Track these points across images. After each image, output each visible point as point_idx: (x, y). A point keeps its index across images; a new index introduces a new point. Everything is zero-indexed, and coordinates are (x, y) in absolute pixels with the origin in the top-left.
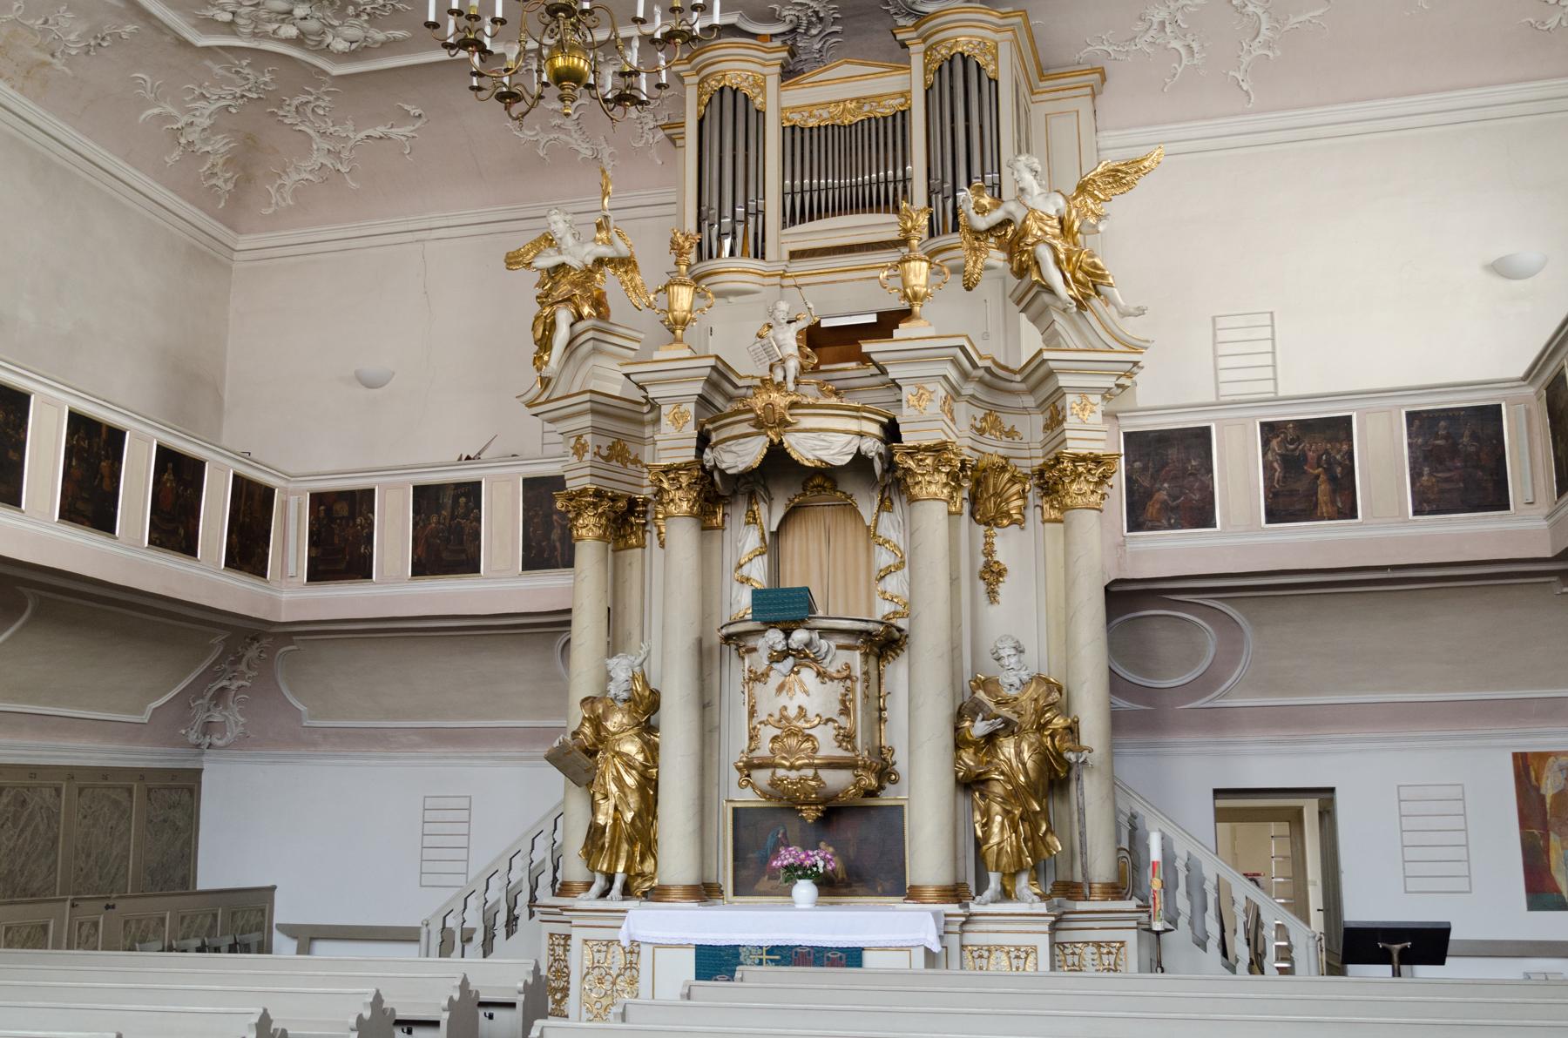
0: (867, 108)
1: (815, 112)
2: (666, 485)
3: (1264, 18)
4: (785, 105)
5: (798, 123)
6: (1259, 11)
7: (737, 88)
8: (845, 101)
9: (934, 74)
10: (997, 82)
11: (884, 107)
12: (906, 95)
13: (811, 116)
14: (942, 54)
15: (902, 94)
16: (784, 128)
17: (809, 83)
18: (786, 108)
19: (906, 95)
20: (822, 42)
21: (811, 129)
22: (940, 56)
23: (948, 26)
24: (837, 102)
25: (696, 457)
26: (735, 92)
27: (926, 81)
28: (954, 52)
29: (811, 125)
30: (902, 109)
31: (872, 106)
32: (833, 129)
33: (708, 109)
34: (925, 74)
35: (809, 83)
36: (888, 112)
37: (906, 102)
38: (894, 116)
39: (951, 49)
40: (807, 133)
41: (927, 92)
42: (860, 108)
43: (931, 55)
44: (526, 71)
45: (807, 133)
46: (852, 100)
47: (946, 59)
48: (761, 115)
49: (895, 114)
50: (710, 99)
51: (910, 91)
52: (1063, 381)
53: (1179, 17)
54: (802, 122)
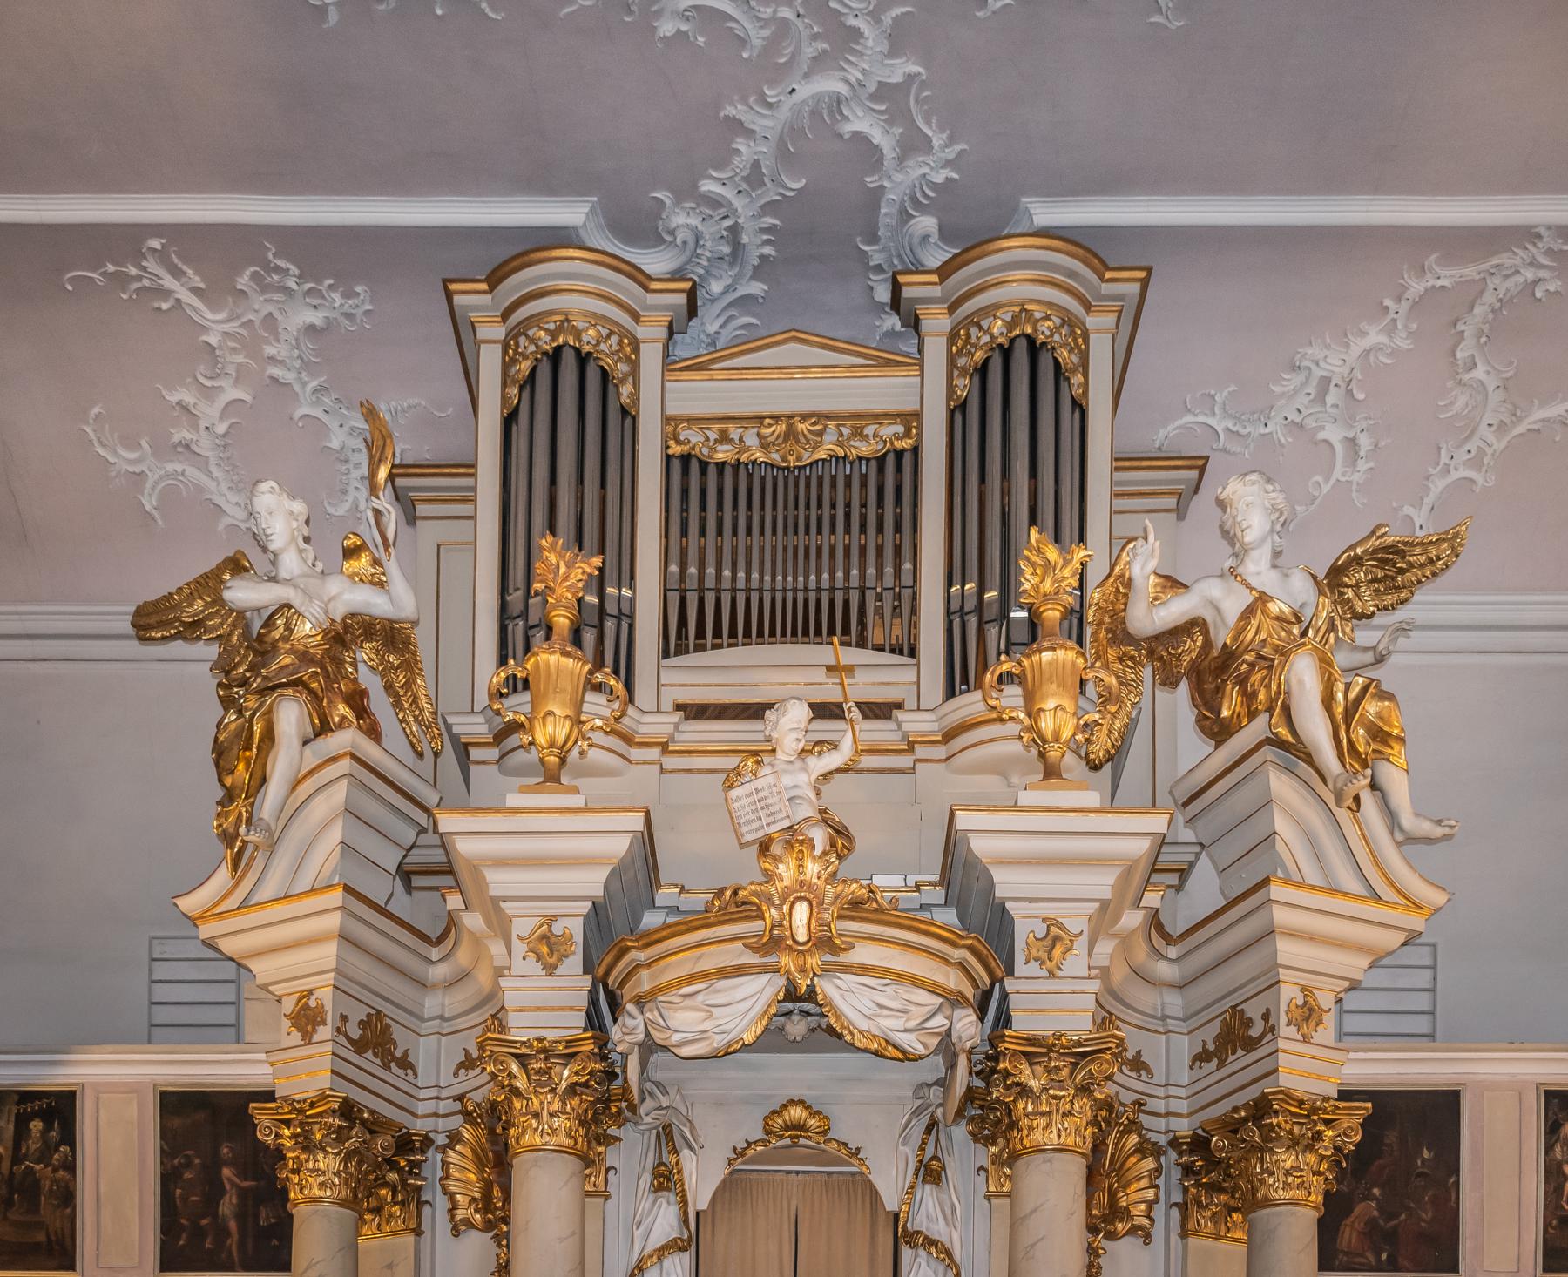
0: (830, 437)
1: (734, 434)
2: (521, 1083)
3: (1495, 397)
4: (670, 412)
6: (1491, 383)
8: (792, 417)
12: (910, 420)
13: (724, 438)
16: (669, 458)
18: (674, 419)
19: (910, 420)
20: (721, 320)
24: (777, 418)
25: (585, 1030)
30: (899, 445)
31: (841, 434)
36: (865, 449)
37: (907, 434)
38: (881, 460)
40: (712, 471)
42: (820, 434)
44: (138, 290)
45: (712, 471)
46: (804, 417)
48: (628, 421)
49: (885, 455)
52: (1287, 950)
53: (1358, 374)
54: (705, 451)
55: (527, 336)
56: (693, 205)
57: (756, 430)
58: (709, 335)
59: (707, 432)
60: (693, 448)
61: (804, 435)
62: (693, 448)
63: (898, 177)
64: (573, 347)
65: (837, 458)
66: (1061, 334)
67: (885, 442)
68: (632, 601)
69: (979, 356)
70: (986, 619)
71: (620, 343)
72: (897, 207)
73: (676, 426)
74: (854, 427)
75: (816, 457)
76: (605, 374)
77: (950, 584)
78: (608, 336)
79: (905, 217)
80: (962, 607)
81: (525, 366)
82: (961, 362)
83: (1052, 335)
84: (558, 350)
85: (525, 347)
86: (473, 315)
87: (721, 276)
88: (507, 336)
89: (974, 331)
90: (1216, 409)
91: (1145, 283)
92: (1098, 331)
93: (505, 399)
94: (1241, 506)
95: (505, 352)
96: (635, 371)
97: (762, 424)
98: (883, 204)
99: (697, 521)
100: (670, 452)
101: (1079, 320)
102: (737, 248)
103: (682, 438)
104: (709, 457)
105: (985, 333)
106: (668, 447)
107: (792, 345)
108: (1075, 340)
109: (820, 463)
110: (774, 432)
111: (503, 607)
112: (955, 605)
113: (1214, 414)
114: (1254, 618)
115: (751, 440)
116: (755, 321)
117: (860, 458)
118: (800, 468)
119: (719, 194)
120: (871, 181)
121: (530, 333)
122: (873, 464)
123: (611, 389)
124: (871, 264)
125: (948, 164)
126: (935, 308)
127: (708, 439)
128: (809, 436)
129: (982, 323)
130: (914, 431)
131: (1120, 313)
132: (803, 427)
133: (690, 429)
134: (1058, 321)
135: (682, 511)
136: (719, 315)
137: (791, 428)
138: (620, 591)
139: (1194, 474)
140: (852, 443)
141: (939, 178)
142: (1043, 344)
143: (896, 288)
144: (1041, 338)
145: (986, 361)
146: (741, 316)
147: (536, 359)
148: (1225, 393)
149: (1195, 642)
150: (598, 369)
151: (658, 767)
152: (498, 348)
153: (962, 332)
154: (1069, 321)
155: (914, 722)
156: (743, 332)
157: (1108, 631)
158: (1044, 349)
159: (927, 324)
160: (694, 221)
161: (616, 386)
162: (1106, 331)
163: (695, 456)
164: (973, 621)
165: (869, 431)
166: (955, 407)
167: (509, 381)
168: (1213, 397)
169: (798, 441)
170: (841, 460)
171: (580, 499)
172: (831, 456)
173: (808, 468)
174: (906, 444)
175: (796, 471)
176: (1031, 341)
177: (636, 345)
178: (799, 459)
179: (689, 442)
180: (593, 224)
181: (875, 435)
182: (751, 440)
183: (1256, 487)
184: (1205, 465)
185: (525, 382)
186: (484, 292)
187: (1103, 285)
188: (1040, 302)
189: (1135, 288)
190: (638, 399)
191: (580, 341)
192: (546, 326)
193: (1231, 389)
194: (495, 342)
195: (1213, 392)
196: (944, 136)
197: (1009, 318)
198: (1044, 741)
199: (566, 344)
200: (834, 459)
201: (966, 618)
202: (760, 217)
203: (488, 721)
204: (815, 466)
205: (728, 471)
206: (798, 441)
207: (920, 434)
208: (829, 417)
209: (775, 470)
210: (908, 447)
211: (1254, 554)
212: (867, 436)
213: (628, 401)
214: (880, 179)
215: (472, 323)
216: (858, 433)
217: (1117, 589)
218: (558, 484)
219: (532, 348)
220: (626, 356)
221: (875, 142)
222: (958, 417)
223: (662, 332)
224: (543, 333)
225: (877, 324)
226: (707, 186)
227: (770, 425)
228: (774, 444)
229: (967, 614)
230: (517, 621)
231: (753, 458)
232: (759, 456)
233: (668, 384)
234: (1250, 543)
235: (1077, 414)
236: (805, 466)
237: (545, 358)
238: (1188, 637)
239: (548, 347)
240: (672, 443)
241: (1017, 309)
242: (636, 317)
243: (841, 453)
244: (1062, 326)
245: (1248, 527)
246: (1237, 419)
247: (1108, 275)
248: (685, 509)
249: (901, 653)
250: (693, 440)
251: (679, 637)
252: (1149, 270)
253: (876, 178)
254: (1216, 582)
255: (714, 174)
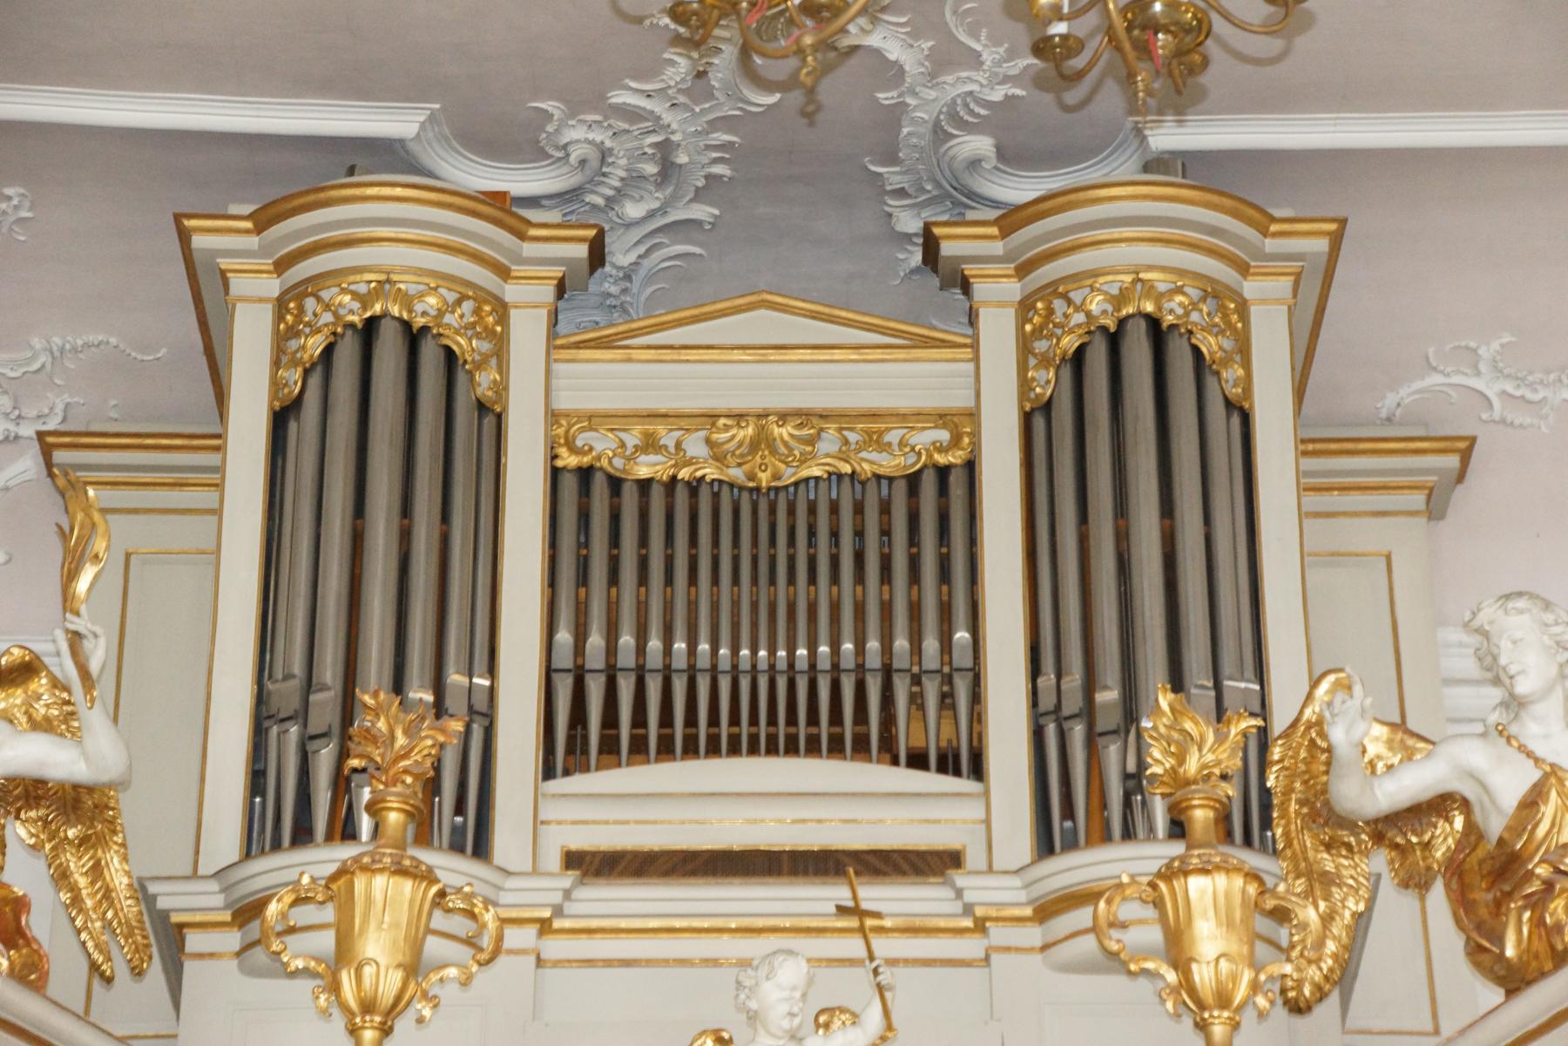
0: (829, 443)
1: (669, 440)
4: (563, 402)
5: (604, 463)
7: (425, 329)
9: (1058, 368)
10: (1246, 419)
11: (885, 447)
13: (650, 444)
14: (1088, 314)
15: (942, 418)
16: (555, 474)
17: (649, 347)
21: (645, 485)
22: (1079, 318)
23: (1116, 232)
24: (739, 417)
26: (413, 337)
27: (1025, 385)
28: (1129, 310)
29: (643, 472)
30: (941, 459)
31: (846, 442)
32: (716, 496)
33: (315, 380)
34: (1023, 367)
35: (649, 347)
36: (889, 463)
37: (956, 441)
38: (913, 481)
39: (1119, 300)
41: (1027, 419)
42: (811, 441)
43: (1050, 312)
46: (783, 417)
47: (1104, 329)
49: (920, 471)
50: (329, 351)
51: (973, 415)
54: (618, 462)
55: (319, 299)
56: (598, 118)
57: (702, 434)
58: (619, 268)
59: (622, 435)
60: (599, 458)
61: (785, 444)
62: (599, 458)
63: (933, 94)
64: (400, 320)
65: (840, 476)
66: (1201, 311)
67: (919, 454)
68: (492, 691)
69: (1070, 343)
70: (1100, 728)
71: (477, 311)
72: (930, 126)
73: (570, 426)
74: (869, 433)
75: (805, 473)
76: (450, 355)
77: (1035, 670)
78: (459, 302)
79: (940, 135)
80: (1058, 706)
81: (314, 345)
82: (1041, 346)
83: (1187, 314)
84: (371, 325)
85: (315, 315)
86: (224, 263)
87: (642, 197)
88: (283, 294)
89: (1058, 304)
90: (1483, 367)
91: (1336, 240)
92: (1263, 301)
93: (276, 384)
94: (1505, 644)
95: (279, 317)
96: (501, 348)
97: (713, 424)
98: (904, 123)
99: (605, 561)
100: (559, 463)
101: (1228, 287)
102: (668, 170)
103: (579, 443)
104: (624, 471)
105: (1078, 309)
106: (555, 457)
107: (762, 312)
108: (1225, 317)
109: (812, 483)
110: (733, 437)
111: (261, 698)
112: (1047, 702)
113: (1478, 374)
114: (1546, 802)
115: (695, 446)
116: (697, 250)
117: (878, 477)
118: (777, 489)
119: (639, 107)
120: (886, 97)
121: (325, 295)
122: (900, 489)
123: (461, 378)
124: (889, 188)
125: (1006, 79)
126: (992, 269)
127: (623, 445)
128: (792, 443)
129: (1072, 295)
130: (966, 440)
131: (1298, 277)
132: (783, 432)
133: (591, 429)
134: (1194, 293)
135: (579, 546)
136: (636, 244)
137: (761, 430)
138: (471, 677)
139: (1453, 461)
140: (864, 454)
141: (997, 95)
142: (1172, 327)
143: (930, 245)
144: (1169, 319)
145: (1080, 352)
146: (674, 243)
147: (334, 334)
148: (1495, 346)
149: (1451, 823)
150: (442, 354)
151: (532, 959)
152: (267, 313)
153: (1039, 305)
154: (1214, 292)
155: (979, 889)
156: (679, 263)
157: (1301, 803)
158: (1176, 333)
159: (980, 289)
160: (597, 136)
161: (470, 373)
162: (1278, 301)
163: (601, 469)
164: (1078, 731)
165: (893, 437)
166: (1033, 410)
167: (284, 359)
168: (1475, 351)
169: (774, 452)
170: (847, 481)
171: (405, 537)
172: (830, 474)
173: (792, 489)
174: (955, 458)
175: (772, 495)
176: (1153, 323)
177: (502, 309)
178: (776, 476)
179: (591, 449)
180: (430, 135)
181: (902, 444)
182: (695, 446)
183: (1526, 617)
184: (1470, 449)
185: (314, 365)
186: (247, 231)
187: (1268, 241)
188: (1163, 269)
189: (1322, 245)
190: (506, 388)
191: (410, 311)
192: (353, 287)
193: (1506, 339)
194: (261, 300)
195: (1473, 344)
196: (1001, 50)
197: (1115, 291)
198: (1202, 1006)
199: (385, 314)
200: (834, 478)
201: (1066, 725)
202: (708, 133)
203: (225, 890)
204: (802, 487)
205: (657, 496)
206: (774, 452)
207: (976, 446)
208: (824, 416)
209: (736, 490)
210: (959, 461)
211: (1538, 709)
212: (890, 444)
213: (490, 393)
214: (899, 96)
215: (223, 273)
216: (875, 441)
217: (1312, 741)
218: (367, 517)
219: (327, 317)
220: (486, 328)
221: (892, 57)
222: (1039, 423)
223: (547, 292)
224: (347, 298)
225: (901, 256)
226: (619, 97)
227: (727, 428)
228: (733, 454)
229: (1067, 718)
230: (287, 724)
231: (699, 474)
232: (711, 472)
233: (556, 367)
234: (1525, 697)
235: (1236, 420)
236: (786, 487)
237: (349, 333)
238: (1439, 816)
239: (355, 319)
240: (563, 451)
241: (1128, 278)
242: (504, 273)
243: (847, 469)
244: (1204, 299)
245: (1519, 673)
246: (1520, 380)
247: (1274, 228)
248: (584, 543)
249: (957, 773)
250: (599, 447)
251: (571, 739)
252: (1343, 222)
253: (895, 94)
254: (1478, 744)
255: (633, 84)
